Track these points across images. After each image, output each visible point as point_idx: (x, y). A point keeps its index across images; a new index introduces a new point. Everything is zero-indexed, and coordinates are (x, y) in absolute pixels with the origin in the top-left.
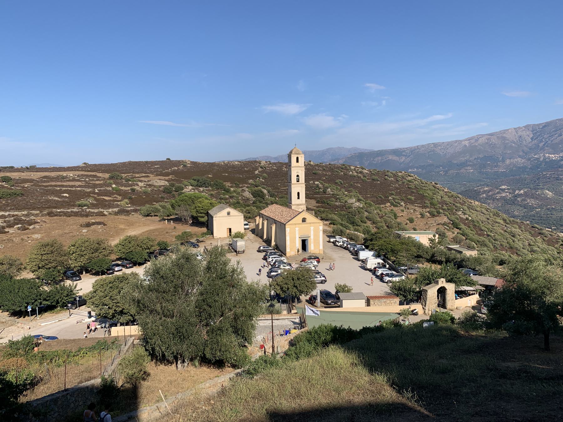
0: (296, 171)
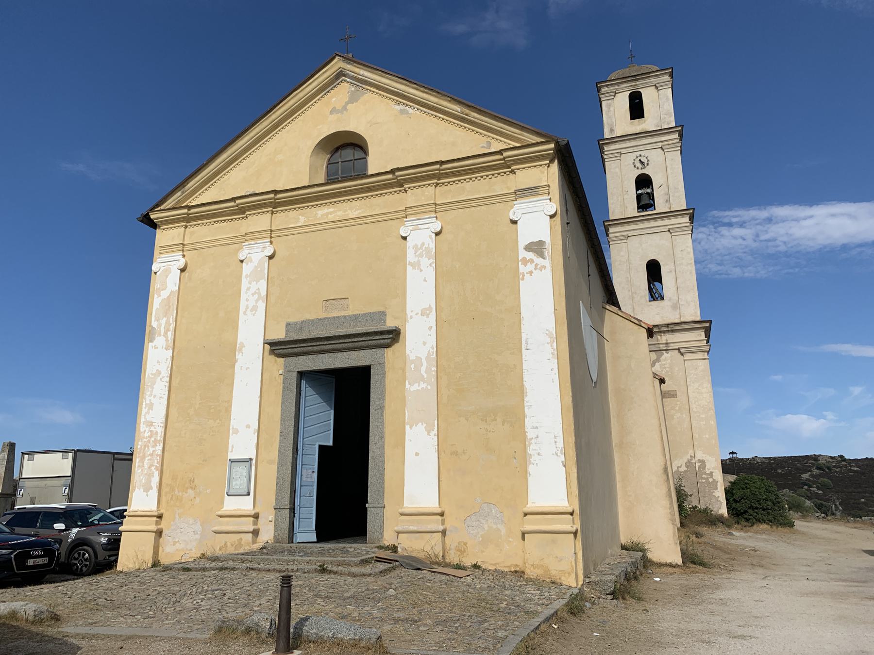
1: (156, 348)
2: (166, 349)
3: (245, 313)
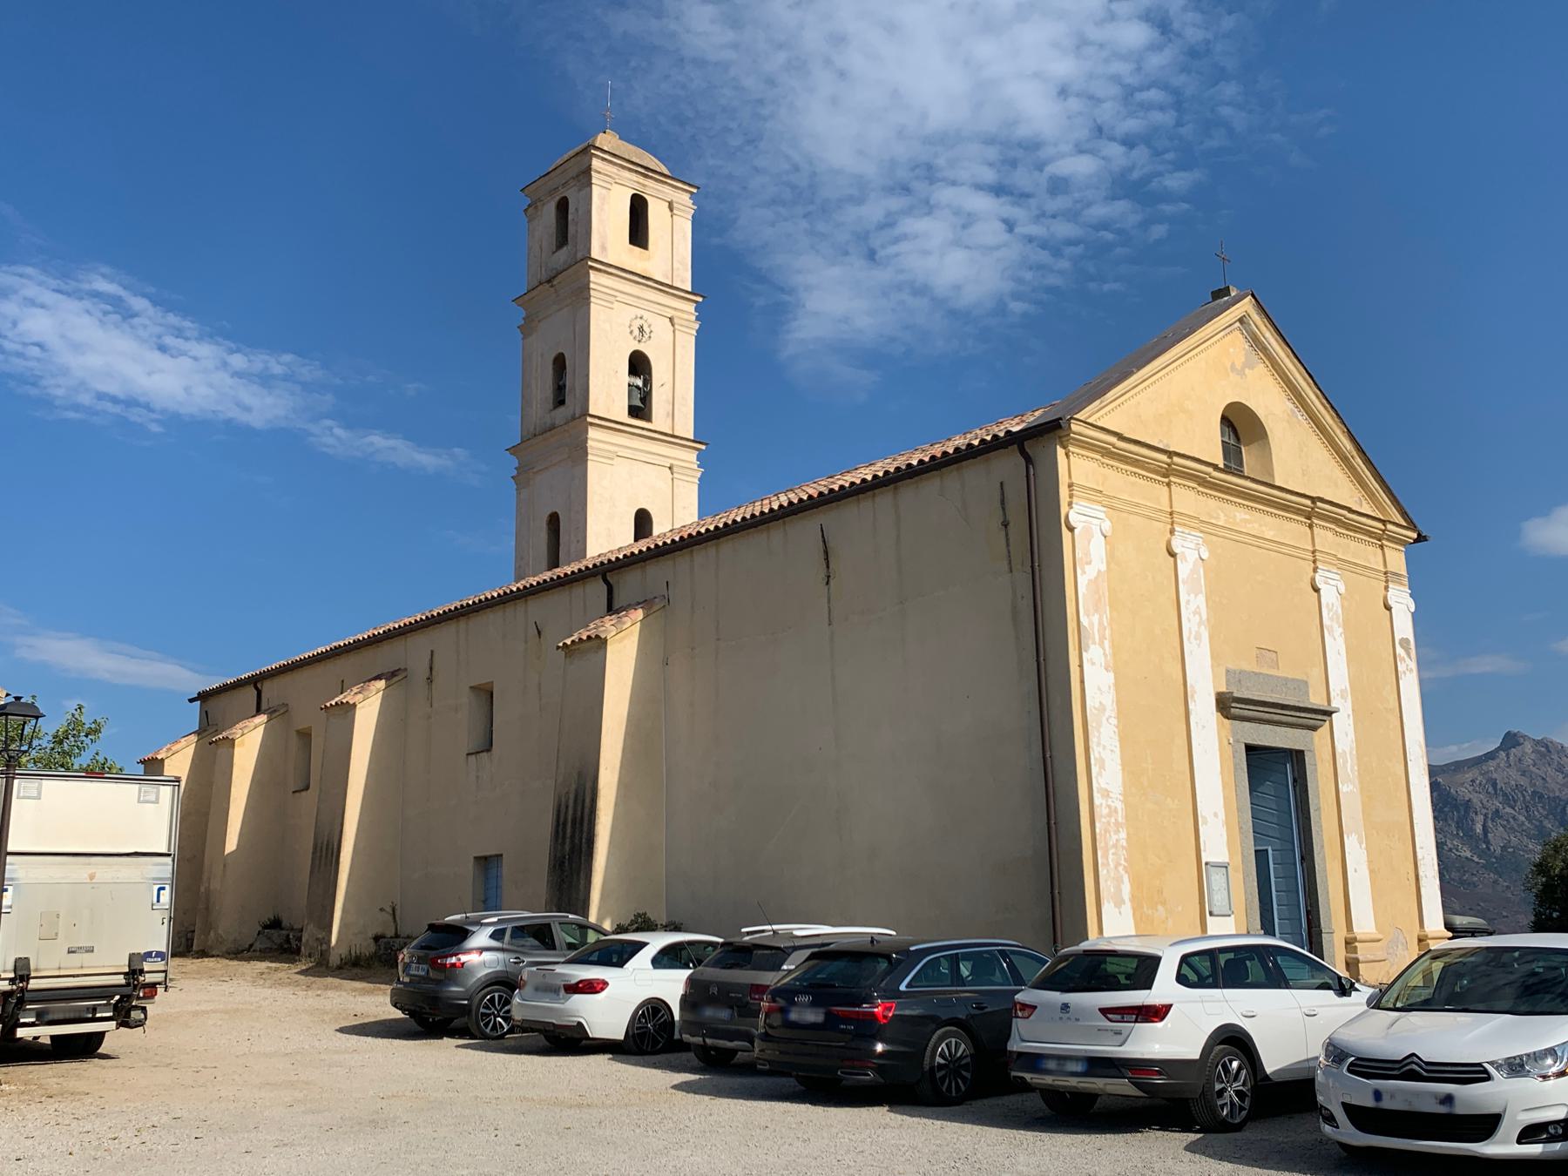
1: (1093, 664)
3: (1189, 639)
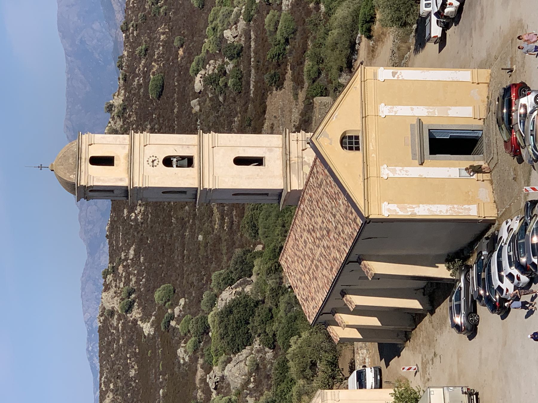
0: (148, 168)
1: (419, 212)
2: (419, 207)
3: (408, 175)
